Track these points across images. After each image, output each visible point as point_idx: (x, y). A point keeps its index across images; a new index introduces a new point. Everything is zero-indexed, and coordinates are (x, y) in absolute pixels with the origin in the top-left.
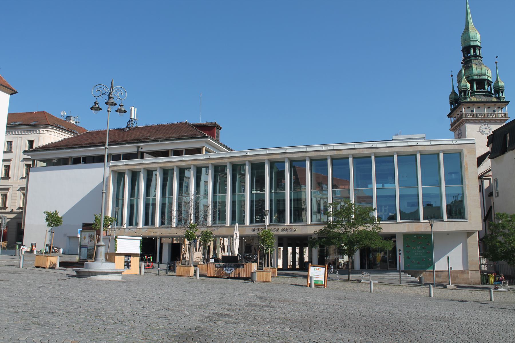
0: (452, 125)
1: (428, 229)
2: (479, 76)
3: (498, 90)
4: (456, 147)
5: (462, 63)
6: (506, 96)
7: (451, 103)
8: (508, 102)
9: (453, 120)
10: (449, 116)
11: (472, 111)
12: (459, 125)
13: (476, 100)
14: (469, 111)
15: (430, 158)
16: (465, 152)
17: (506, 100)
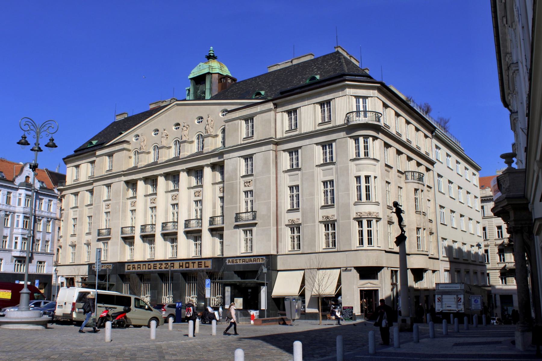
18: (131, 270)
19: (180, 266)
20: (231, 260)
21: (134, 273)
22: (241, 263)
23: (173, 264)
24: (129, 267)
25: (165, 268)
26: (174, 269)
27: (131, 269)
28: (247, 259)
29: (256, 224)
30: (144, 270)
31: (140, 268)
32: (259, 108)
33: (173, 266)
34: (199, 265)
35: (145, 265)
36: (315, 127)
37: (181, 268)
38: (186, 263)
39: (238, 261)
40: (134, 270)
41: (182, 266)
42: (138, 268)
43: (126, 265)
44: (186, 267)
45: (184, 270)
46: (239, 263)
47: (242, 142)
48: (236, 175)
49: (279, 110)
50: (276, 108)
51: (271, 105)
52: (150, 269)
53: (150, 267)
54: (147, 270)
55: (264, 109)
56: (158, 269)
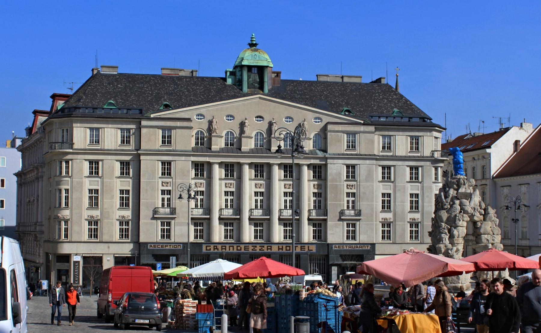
18: (212, 250)
19: (279, 249)
20: (337, 246)
21: (216, 253)
22: (348, 248)
23: (271, 247)
24: (208, 248)
25: (260, 250)
26: (272, 251)
27: (212, 250)
28: (353, 245)
29: (360, 219)
30: (231, 251)
31: (225, 249)
32: (362, 128)
33: (271, 249)
34: (301, 248)
35: (233, 247)
36: (407, 154)
37: (281, 251)
38: (286, 247)
39: (345, 247)
40: (216, 251)
41: (282, 249)
42: (222, 249)
43: (204, 247)
44: (286, 250)
45: (284, 253)
46: (345, 248)
47: (345, 152)
48: (340, 178)
49: (377, 133)
50: (375, 131)
51: (372, 128)
52: (241, 250)
53: (239, 248)
54: (235, 250)
55: (367, 130)
56: (250, 251)
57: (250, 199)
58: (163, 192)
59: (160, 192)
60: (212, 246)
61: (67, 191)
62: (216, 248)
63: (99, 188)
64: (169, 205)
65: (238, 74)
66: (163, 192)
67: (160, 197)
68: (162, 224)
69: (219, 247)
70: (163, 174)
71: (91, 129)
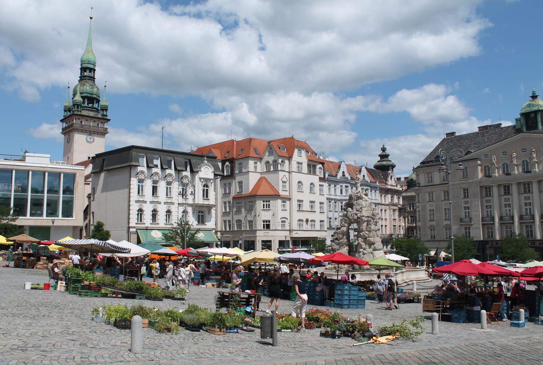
0: (63, 129)
1: (50, 224)
2: (91, 94)
3: (105, 109)
4: (73, 171)
5: (89, 158)
6: (110, 114)
7: (65, 111)
8: (109, 120)
9: (65, 125)
10: (62, 121)
11: (81, 122)
12: (70, 131)
13: (85, 114)
14: (79, 122)
15: (55, 175)
16: (77, 175)
17: (108, 118)
18: (495, 245)
19: (540, 244)
33: (534, 244)
57: (520, 208)
58: (465, 208)
59: (463, 209)
60: (495, 243)
61: (419, 211)
62: (497, 243)
63: (434, 208)
64: (469, 216)
65: (521, 120)
66: (465, 208)
67: (464, 211)
68: (466, 228)
69: (499, 243)
70: (465, 196)
71: (428, 173)
